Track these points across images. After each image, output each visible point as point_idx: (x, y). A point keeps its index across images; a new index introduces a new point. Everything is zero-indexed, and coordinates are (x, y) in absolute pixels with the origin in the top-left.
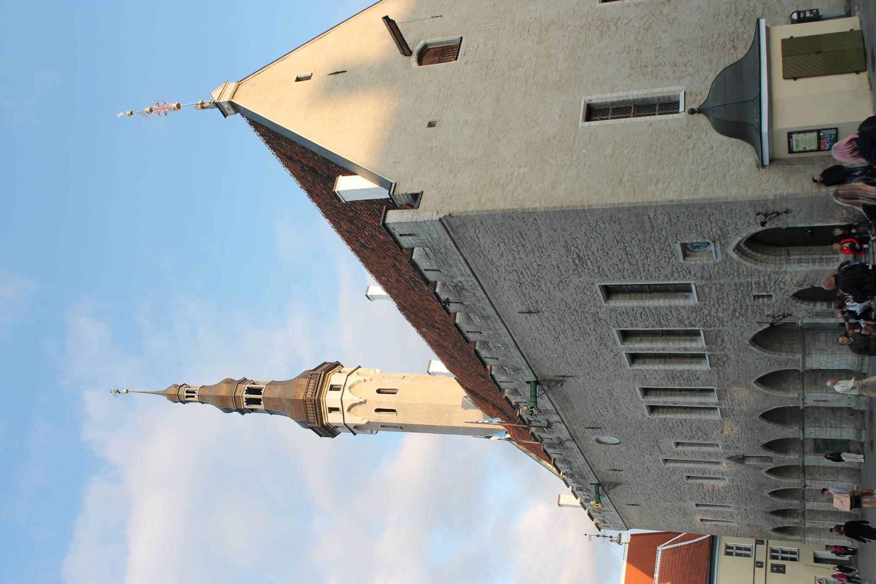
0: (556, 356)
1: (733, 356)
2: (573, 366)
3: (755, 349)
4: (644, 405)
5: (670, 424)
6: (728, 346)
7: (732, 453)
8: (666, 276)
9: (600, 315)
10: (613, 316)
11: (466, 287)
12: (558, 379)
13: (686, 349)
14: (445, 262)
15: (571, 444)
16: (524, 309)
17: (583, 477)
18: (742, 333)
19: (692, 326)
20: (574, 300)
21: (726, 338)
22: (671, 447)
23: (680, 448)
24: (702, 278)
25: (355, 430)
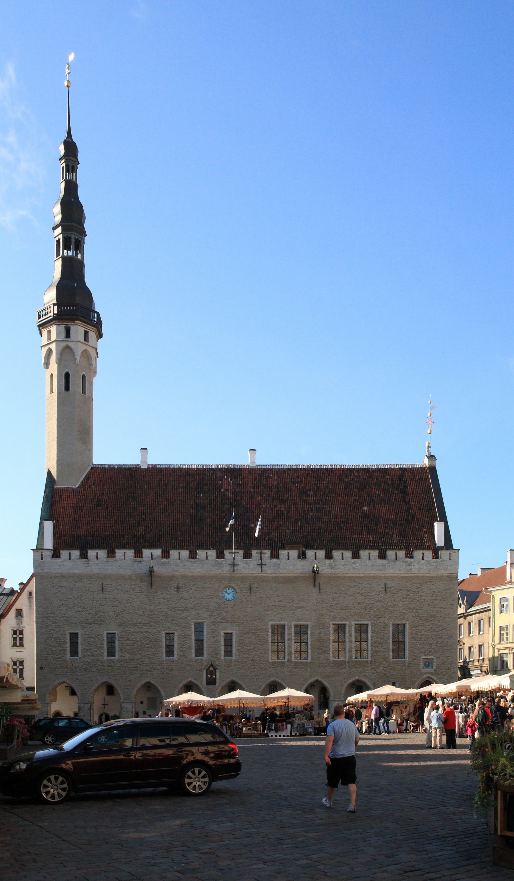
0: (343, 589)
1: (343, 670)
2: (333, 595)
3: (351, 681)
4: (286, 623)
5: (259, 633)
6: (353, 669)
7: (217, 663)
8: (412, 650)
9: (382, 619)
10: (381, 624)
11: (410, 567)
12: (317, 584)
13: (350, 651)
14: (430, 564)
15: (225, 570)
16: (387, 586)
17: (165, 564)
18: (366, 676)
19: (372, 656)
20: (396, 610)
21: (360, 669)
22: (225, 629)
23: (222, 634)
24: (410, 664)
25: (64, 344)
